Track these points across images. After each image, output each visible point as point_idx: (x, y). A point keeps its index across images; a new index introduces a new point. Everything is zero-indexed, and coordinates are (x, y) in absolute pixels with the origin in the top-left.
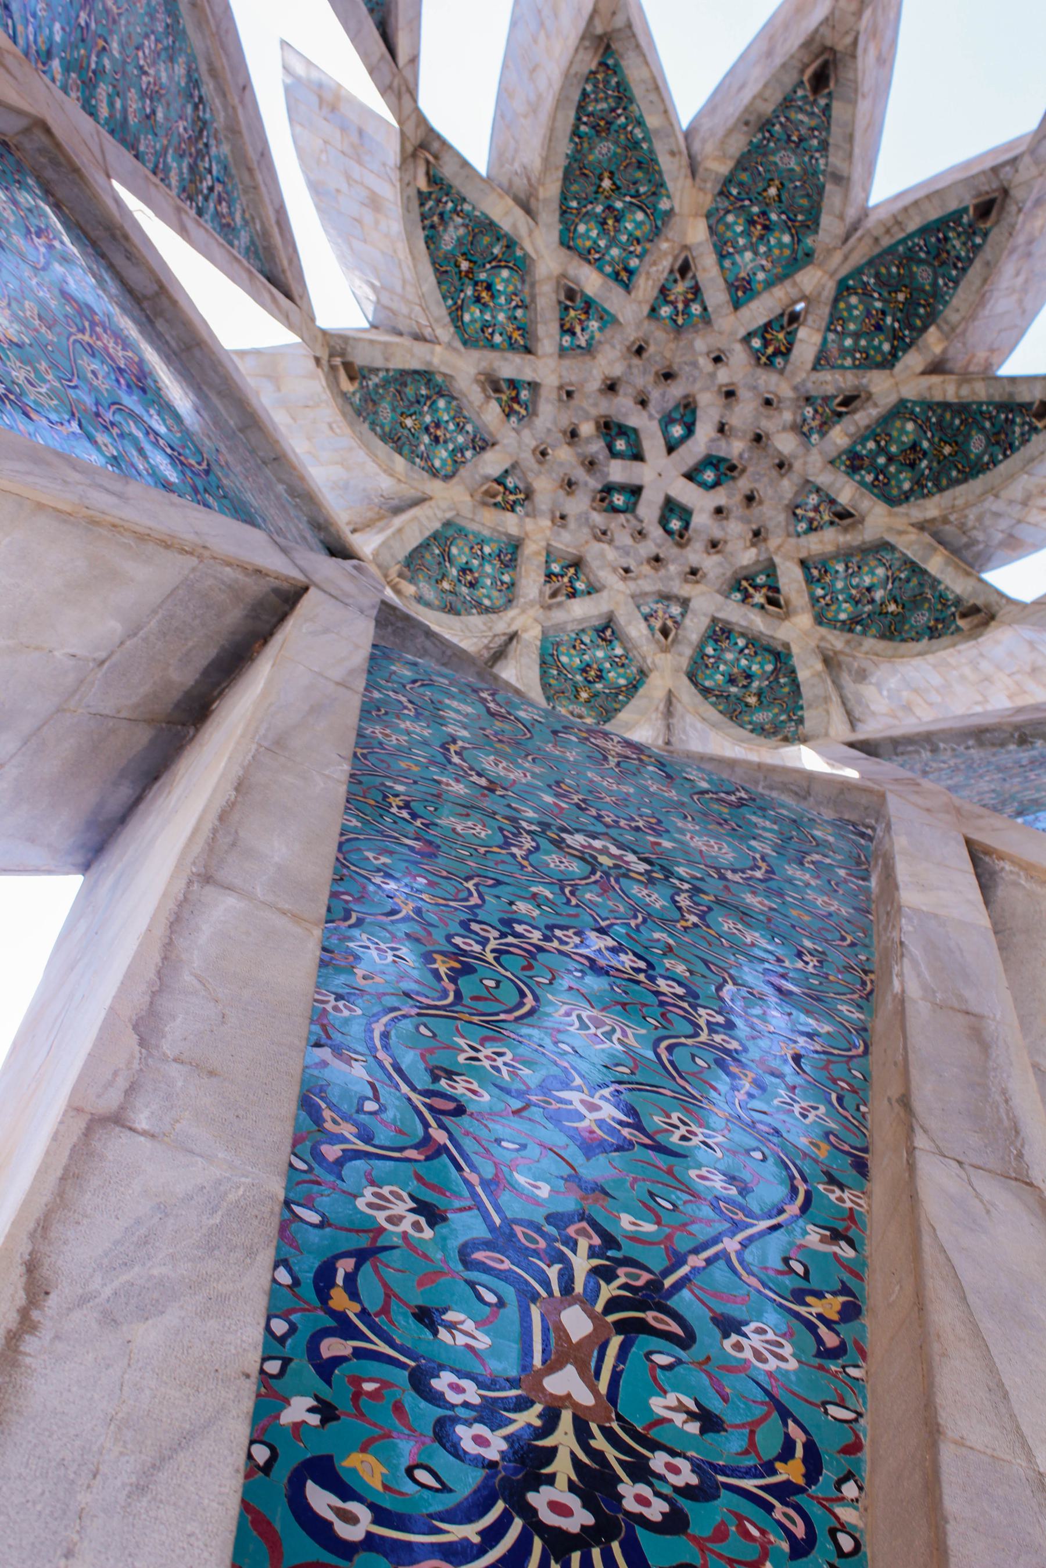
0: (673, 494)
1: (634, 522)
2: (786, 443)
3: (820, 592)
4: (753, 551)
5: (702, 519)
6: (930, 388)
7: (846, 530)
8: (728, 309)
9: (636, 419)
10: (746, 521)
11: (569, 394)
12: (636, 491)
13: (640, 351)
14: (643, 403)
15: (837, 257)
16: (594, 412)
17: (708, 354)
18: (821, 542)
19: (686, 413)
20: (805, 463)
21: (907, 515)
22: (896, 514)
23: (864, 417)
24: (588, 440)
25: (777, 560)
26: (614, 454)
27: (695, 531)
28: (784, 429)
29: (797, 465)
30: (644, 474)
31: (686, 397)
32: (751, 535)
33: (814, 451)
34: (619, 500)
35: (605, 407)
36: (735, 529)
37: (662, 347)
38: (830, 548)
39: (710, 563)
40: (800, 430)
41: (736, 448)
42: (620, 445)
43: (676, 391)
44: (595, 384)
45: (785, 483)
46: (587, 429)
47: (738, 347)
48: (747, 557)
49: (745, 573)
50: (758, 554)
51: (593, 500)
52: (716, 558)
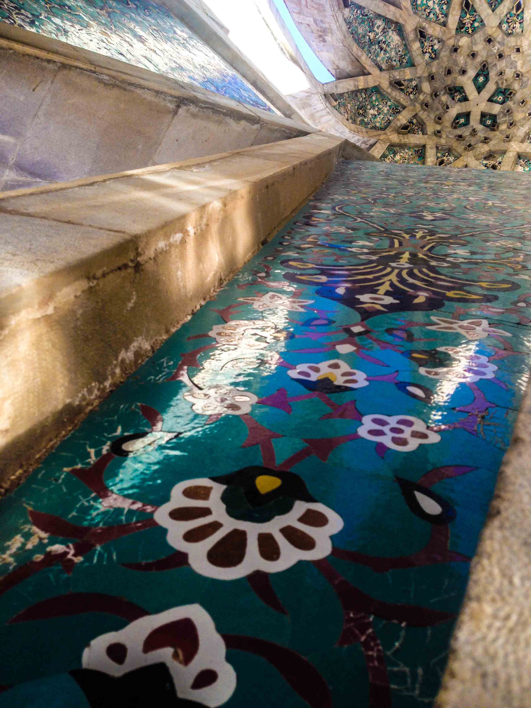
0: (476, 93)
1: (500, 82)
2: (426, 87)
3: (445, 7)
4: (460, 44)
5: (472, 73)
6: (370, 66)
7: (424, 28)
8: (428, 147)
9: (479, 127)
10: (455, 62)
11: (508, 137)
12: (490, 100)
13: (470, 146)
14: (474, 130)
15: (382, 137)
16: (497, 133)
17: (440, 137)
18: (434, 30)
19: (455, 125)
20: (424, 72)
21: (401, 15)
22: (404, 20)
23: (397, 75)
24: (505, 122)
25: (454, 32)
26: (494, 117)
27: (476, 68)
28: (425, 93)
29: (426, 75)
30: (484, 106)
31: (455, 128)
32: (459, 50)
33: (418, 75)
34: (500, 98)
35: (491, 134)
36: (461, 59)
37: (459, 147)
38: (433, 24)
39: (480, 47)
40: (417, 89)
41: (445, 98)
42: (489, 122)
43: (458, 132)
44: (492, 142)
45: (434, 70)
46: (503, 127)
47: (429, 133)
48: (464, 41)
49: (469, 36)
50: (459, 41)
51: (514, 94)
52: (475, 49)
